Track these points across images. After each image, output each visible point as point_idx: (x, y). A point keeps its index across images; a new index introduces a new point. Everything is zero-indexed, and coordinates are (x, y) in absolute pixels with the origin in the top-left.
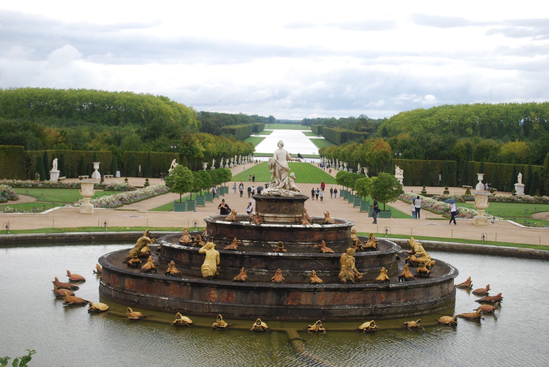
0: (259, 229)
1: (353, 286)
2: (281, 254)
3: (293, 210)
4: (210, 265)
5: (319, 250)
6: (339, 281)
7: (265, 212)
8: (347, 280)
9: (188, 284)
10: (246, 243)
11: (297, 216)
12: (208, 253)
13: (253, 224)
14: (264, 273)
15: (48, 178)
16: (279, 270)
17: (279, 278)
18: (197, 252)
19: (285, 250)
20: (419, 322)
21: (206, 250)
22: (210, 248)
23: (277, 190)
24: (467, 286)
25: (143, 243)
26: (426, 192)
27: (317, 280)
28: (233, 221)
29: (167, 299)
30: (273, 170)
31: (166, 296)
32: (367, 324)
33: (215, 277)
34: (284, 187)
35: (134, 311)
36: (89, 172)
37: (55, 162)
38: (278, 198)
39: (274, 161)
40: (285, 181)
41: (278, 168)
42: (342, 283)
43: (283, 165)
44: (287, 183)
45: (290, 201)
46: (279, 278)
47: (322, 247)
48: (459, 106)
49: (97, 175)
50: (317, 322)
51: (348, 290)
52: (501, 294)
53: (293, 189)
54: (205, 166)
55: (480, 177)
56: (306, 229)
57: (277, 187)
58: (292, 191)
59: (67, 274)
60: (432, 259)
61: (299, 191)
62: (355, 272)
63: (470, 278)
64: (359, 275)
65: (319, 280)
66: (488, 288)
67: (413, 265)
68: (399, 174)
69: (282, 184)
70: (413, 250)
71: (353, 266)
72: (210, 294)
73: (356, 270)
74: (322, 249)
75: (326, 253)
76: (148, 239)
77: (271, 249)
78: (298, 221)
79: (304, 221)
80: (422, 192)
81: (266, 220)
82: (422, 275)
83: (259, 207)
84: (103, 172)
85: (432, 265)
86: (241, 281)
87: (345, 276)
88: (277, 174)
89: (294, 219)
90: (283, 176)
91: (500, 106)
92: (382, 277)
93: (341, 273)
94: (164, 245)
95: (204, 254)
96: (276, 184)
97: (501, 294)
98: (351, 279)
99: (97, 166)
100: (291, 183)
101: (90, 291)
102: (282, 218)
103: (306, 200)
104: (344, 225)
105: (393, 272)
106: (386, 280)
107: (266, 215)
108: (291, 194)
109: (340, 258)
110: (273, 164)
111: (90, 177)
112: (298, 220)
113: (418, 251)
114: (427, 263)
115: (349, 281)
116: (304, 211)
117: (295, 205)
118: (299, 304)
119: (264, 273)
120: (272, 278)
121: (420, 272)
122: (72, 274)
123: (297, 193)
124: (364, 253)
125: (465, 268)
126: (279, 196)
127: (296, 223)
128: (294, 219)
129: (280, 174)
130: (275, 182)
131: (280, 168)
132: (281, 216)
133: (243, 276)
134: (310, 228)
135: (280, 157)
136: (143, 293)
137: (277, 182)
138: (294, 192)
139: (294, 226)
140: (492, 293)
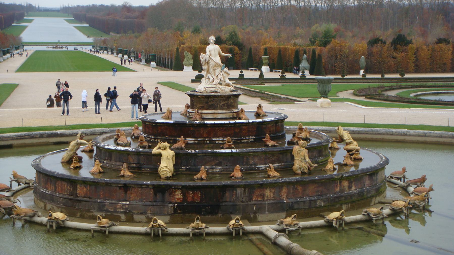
2: (234, 150)
3: (230, 105)
4: (166, 166)
7: (203, 108)
8: (302, 172)
10: (190, 140)
11: (234, 111)
12: (163, 153)
13: (198, 122)
14: (218, 170)
16: (238, 167)
18: (150, 155)
21: (160, 151)
22: (165, 149)
23: (214, 86)
29: (128, 203)
31: (126, 201)
38: (216, 94)
39: (208, 57)
40: (220, 77)
41: (212, 63)
42: (298, 174)
43: (216, 61)
45: (229, 97)
46: (238, 174)
47: (267, 141)
50: (293, 216)
57: (214, 83)
58: (228, 87)
62: (310, 165)
64: (311, 166)
66: (404, 170)
69: (217, 81)
71: (308, 159)
72: (175, 195)
73: (310, 161)
81: (204, 116)
86: (202, 179)
87: (300, 168)
88: (211, 70)
96: (211, 80)
97: (425, 176)
98: (306, 171)
107: (205, 111)
109: (292, 150)
110: (207, 60)
115: (303, 173)
120: (232, 175)
132: (220, 111)
133: (202, 174)
135: (213, 53)
136: (100, 199)
137: (211, 79)
138: (230, 88)
139: (238, 121)
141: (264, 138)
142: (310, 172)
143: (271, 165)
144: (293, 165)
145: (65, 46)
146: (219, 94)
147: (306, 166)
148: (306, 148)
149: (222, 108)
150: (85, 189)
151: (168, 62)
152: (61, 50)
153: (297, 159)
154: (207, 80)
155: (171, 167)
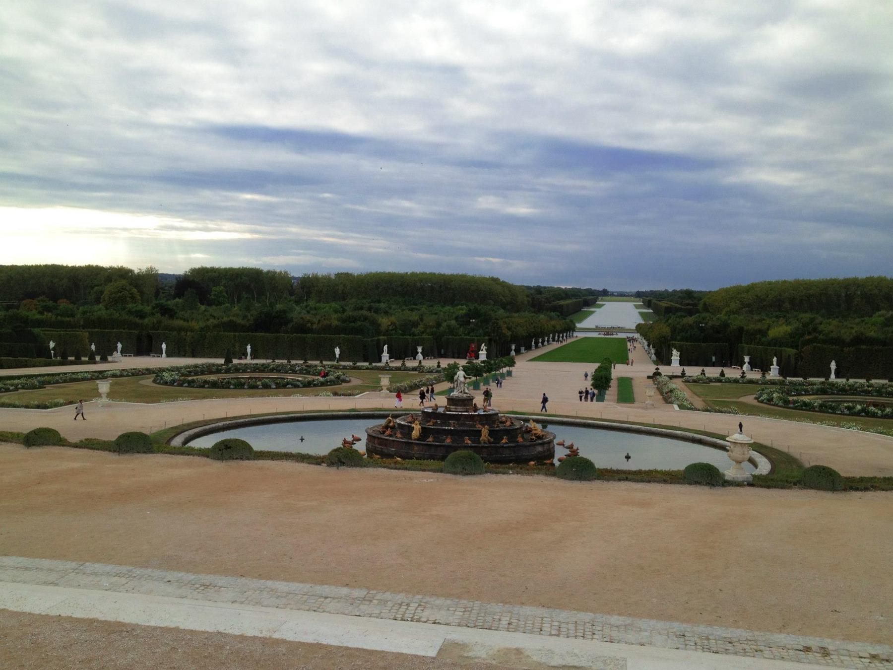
4: (415, 433)
5: (475, 426)
6: (480, 443)
10: (439, 421)
15: (380, 361)
33: (418, 439)
36: (414, 355)
37: (386, 347)
48: (777, 282)
49: (420, 356)
54: (513, 347)
55: (747, 359)
65: (469, 442)
68: (676, 356)
84: (425, 355)
91: (819, 282)
99: (420, 349)
102: (459, 409)
108: (465, 395)
111: (415, 359)
155: (418, 434)
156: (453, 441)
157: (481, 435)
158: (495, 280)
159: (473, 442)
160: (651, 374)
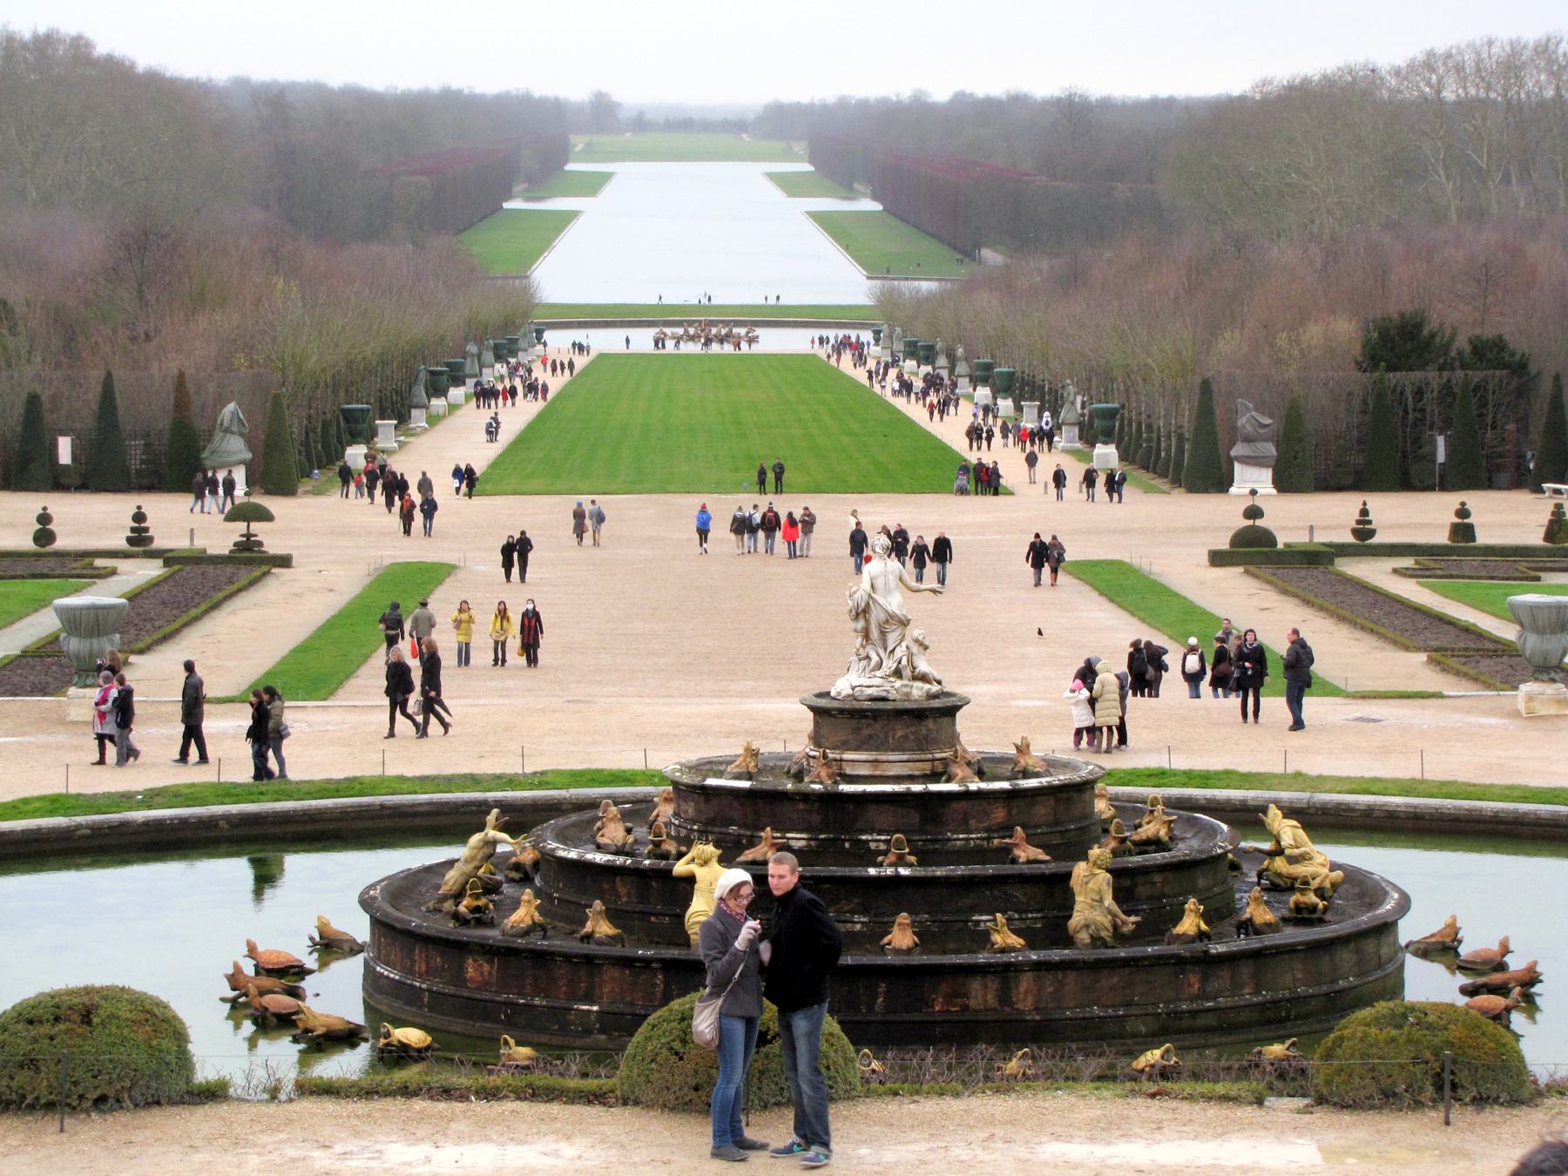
0: (831, 799)
1: (1109, 953)
2: (904, 871)
3: (926, 737)
5: (1005, 854)
6: (1068, 941)
7: (845, 746)
9: (654, 965)
11: (938, 756)
12: (700, 873)
13: (817, 787)
14: (858, 927)
16: (903, 918)
17: (901, 937)
18: (666, 874)
19: (913, 859)
20: (1293, 1044)
21: (693, 868)
22: (705, 863)
24: (1442, 949)
25: (487, 851)
26: (1372, 533)
27: (1009, 941)
28: (750, 777)
29: (595, 1008)
30: (861, 624)
31: (592, 1003)
32: (1153, 1056)
34: (898, 673)
35: (518, 1044)
39: (865, 597)
40: (899, 653)
41: (876, 616)
44: (904, 662)
45: (918, 715)
46: (901, 937)
47: (1016, 845)
51: (1098, 966)
52: (1535, 963)
53: (924, 678)
56: (967, 795)
57: (878, 673)
58: (920, 684)
59: (245, 951)
60: (1334, 867)
61: (939, 682)
62: (1115, 916)
63: (1454, 919)
64: (1124, 923)
66: (1505, 950)
67: (1278, 887)
69: (889, 665)
70: (1278, 842)
71: (1109, 901)
73: (1115, 908)
74: (1017, 852)
75: (1029, 862)
76: (505, 836)
77: (871, 858)
78: (940, 769)
79: (959, 771)
80: (1355, 532)
81: (848, 771)
82: (1303, 916)
83: (824, 731)
85: (1334, 886)
87: (1087, 926)
88: (875, 634)
89: (928, 766)
90: (892, 639)
92: (1189, 924)
93: (1076, 920)
94: (561, 853)
95: (690, 880)
97: (1535, 963)
98: (1104, 934)
100: (915, 659)
101: (337, 994)
102: (896, 762)
103: (960, 707)
104: (1075, 777)
105: (1220, 912)
106: (1201, 935)
107: (848, 756)
108: (918, 690)
109: (1068, 875)
112: (939, 767)
113: (1291, 847)
114: (1318, 881)
115: (1097, 941)
116: (953, 740)
117: (930, 724)
118: (965, 1008)
119: (858, 927)
120: (886, 940)
121: (1298, 908)
122: (261, 948)
123: (935, 688)
124: (1136, 860)
125: (1437, 890)
126: (884, 699)
127: (935, 777)
128: (928, 766)
129: (883, 634)
130: (868, 657)
131: (883, 617)
134: (980, 794)
135: (880, 583)
136: (523, 995)
137: (875, 658)
138: (927, 686)
139: (934, 787)
140: (1515, 963)
141: (1011, 837)
142: (1120, 937)
143: (999, 915)
144: (1070, 917)
145: (742, 331)
146: (889, 706)
147: (1106, 921)
148: (1108, 871)
149: (899, 748)
150: (486, 967)
151: (1168, 450)
152: (728, 348)
153: (1080, 899)
154: (864, 663)
156: (925, 938)
157: (1066, 903)
158: (80, 47)
159: (1032, 940)
160: (1223, 544)
